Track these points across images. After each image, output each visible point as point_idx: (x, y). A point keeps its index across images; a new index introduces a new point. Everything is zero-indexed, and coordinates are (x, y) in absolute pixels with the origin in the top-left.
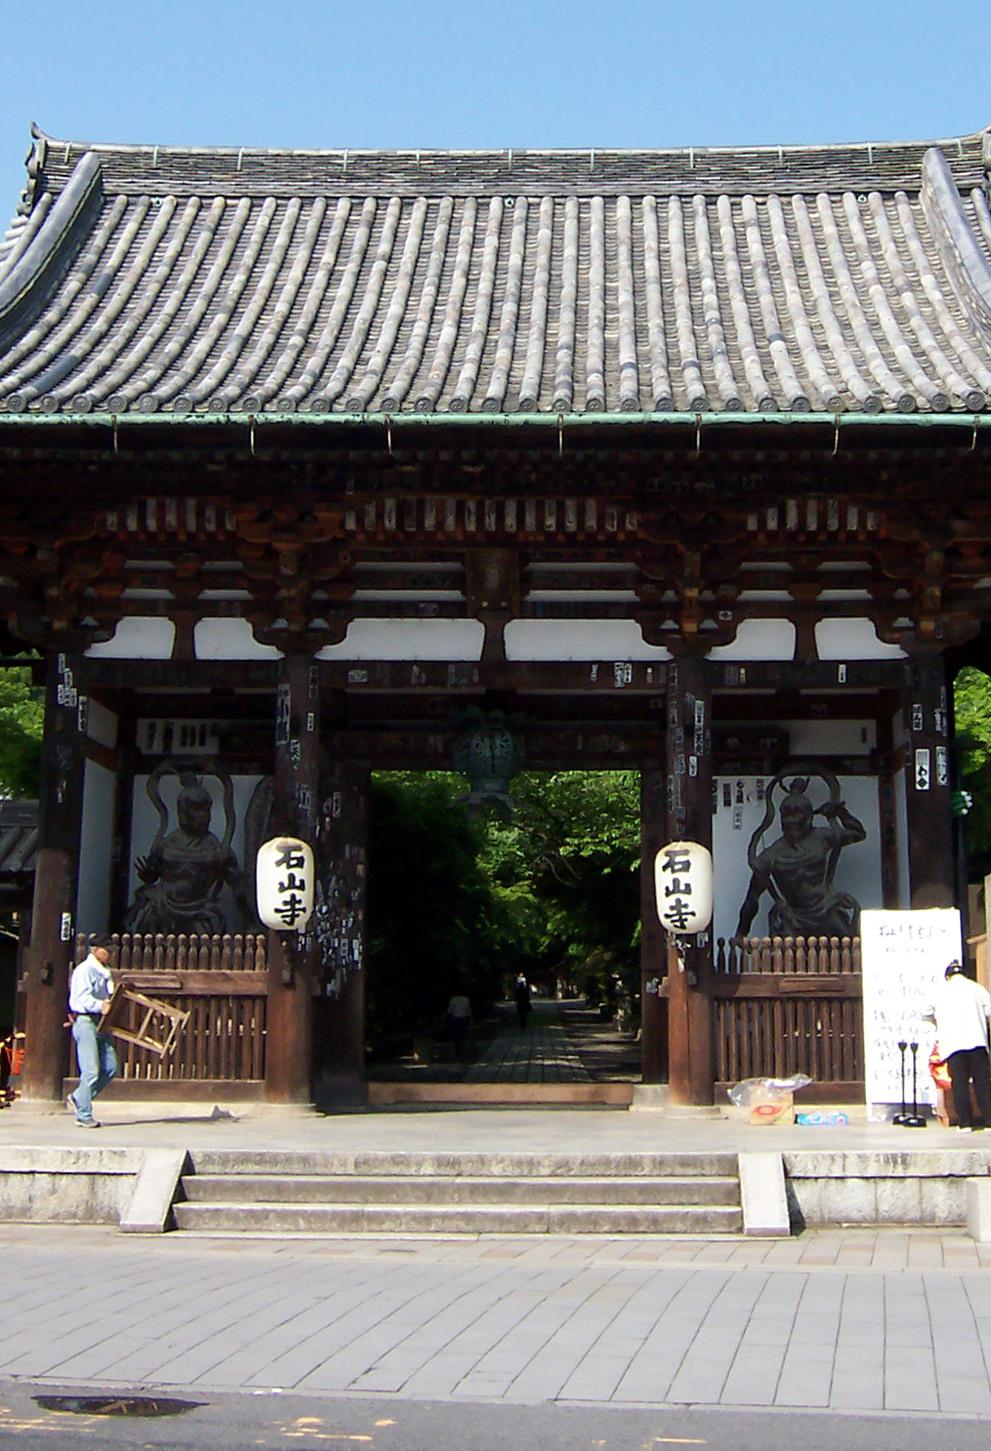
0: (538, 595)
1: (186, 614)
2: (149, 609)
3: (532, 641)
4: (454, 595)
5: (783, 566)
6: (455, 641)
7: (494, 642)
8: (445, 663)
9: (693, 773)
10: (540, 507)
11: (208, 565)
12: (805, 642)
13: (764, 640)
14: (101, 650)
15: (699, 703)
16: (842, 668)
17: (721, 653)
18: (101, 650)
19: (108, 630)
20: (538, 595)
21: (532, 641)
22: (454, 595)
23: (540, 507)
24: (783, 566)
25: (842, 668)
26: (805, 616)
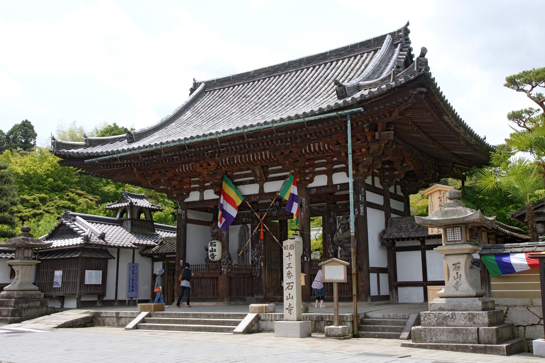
0: (271, 176)
1: (202, 189)
2: (195, 189)
3: (270, 187)
4: (252, 178)
5: (324, 161)
6: (252, 189)
7: (261, 188)
8: (251, 195)
9: (302, 217)
10: (257, 155)
11: (192, 179)
12: (330, 180)
13: (320, 181)
14: (187, 200)
15: (304, 199)
16: (339, 186)
17: (310, 185)
18: (187, 200)
19: (188, 195)
20: (271, 176)
21: (270, 187)
22: (252, 178)
23: (257, 155)
24: (324, 161)
25: (339, 186)
26: (329, 173)
